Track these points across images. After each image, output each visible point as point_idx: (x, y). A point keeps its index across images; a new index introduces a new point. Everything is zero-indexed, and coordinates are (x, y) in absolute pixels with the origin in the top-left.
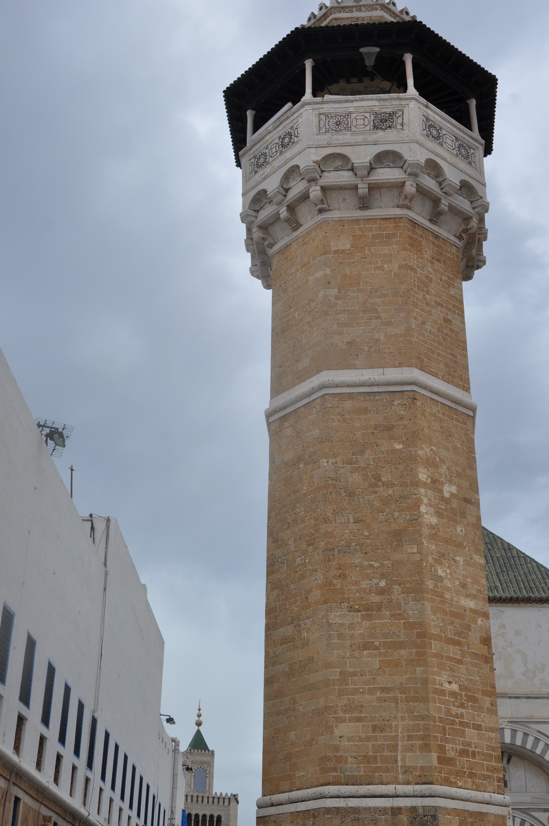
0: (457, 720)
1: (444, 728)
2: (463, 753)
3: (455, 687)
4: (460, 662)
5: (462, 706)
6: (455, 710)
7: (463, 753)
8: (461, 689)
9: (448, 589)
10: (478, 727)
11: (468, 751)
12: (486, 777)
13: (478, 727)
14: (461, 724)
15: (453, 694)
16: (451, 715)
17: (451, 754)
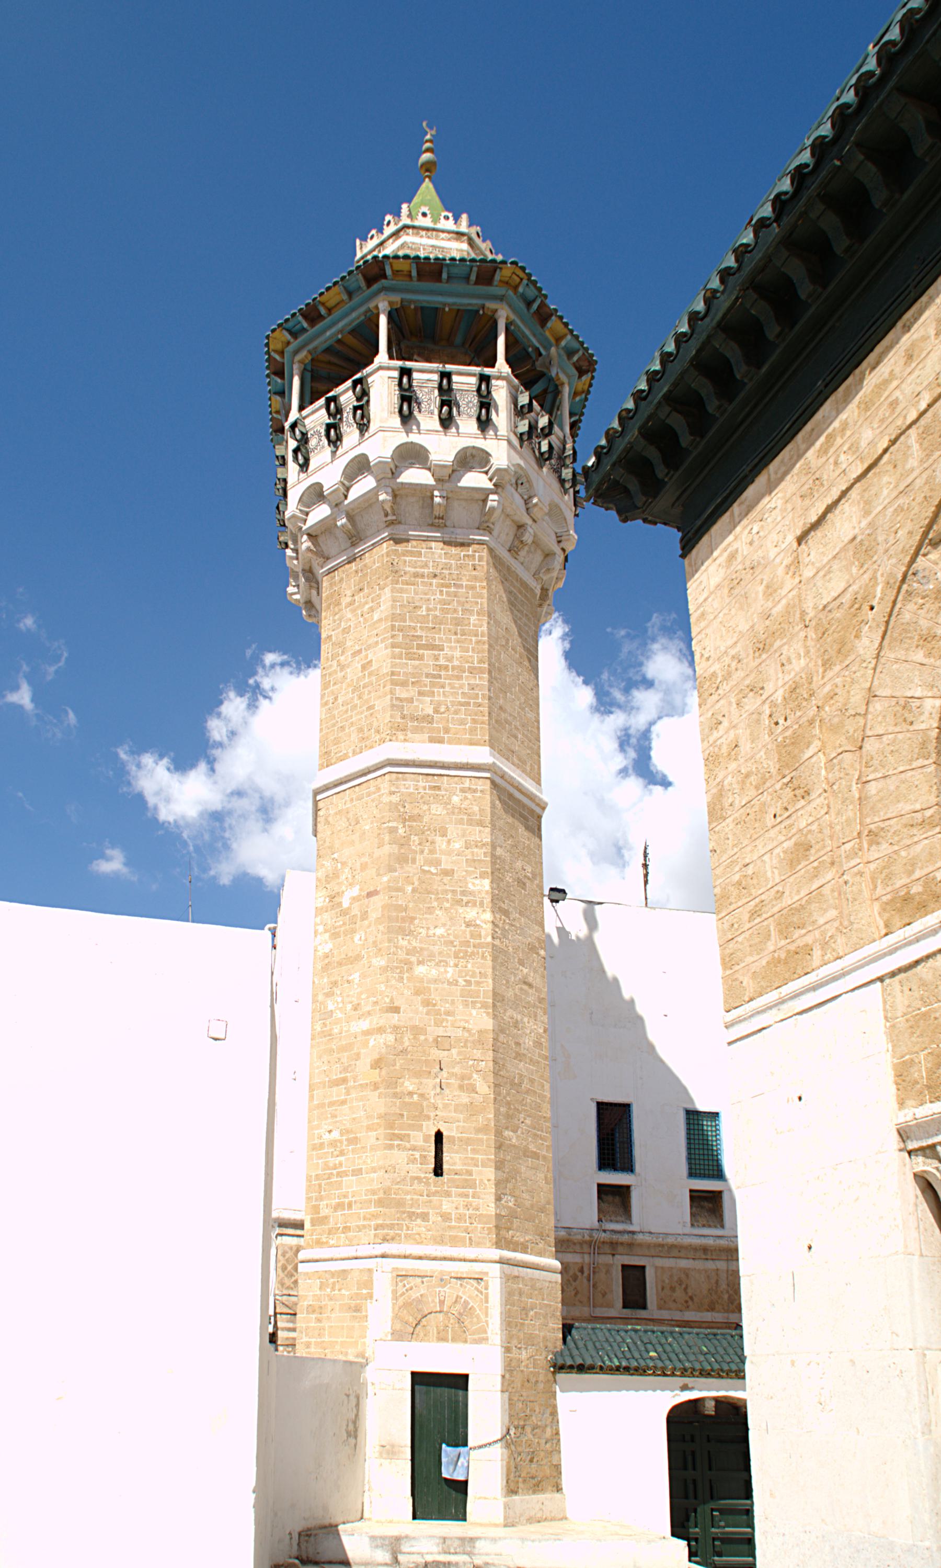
0: (335, 1172)
1: (320, 1185)
2: (339, 1206)
3: (336, 1135)
4: (343, 1102)
5: (342, 1153)
6: (332, 1161)
7: (339, 1206)
8: (342, 1135)
9: (338, 1021)
10: (358, 1172)
11: (343, 1203)
12: (360, 1229)
13: (358, 1172)
14: (339, 1174)
15: (333, 1143)
16: (329, 1169)
17: (324, 1212)
